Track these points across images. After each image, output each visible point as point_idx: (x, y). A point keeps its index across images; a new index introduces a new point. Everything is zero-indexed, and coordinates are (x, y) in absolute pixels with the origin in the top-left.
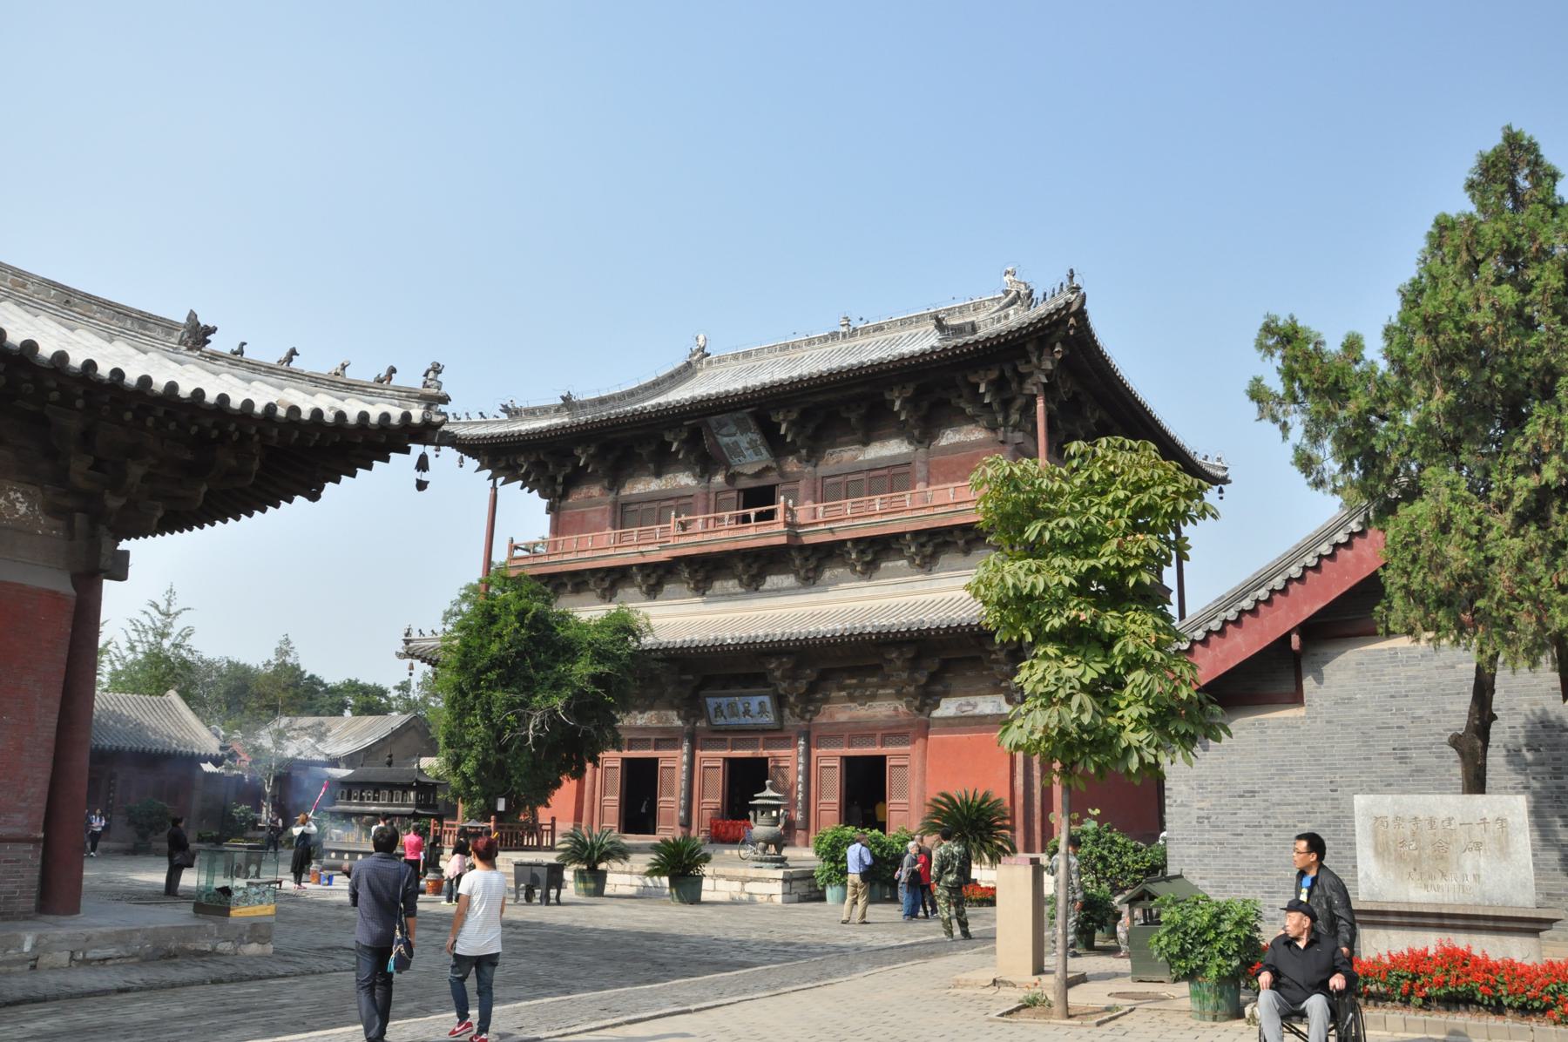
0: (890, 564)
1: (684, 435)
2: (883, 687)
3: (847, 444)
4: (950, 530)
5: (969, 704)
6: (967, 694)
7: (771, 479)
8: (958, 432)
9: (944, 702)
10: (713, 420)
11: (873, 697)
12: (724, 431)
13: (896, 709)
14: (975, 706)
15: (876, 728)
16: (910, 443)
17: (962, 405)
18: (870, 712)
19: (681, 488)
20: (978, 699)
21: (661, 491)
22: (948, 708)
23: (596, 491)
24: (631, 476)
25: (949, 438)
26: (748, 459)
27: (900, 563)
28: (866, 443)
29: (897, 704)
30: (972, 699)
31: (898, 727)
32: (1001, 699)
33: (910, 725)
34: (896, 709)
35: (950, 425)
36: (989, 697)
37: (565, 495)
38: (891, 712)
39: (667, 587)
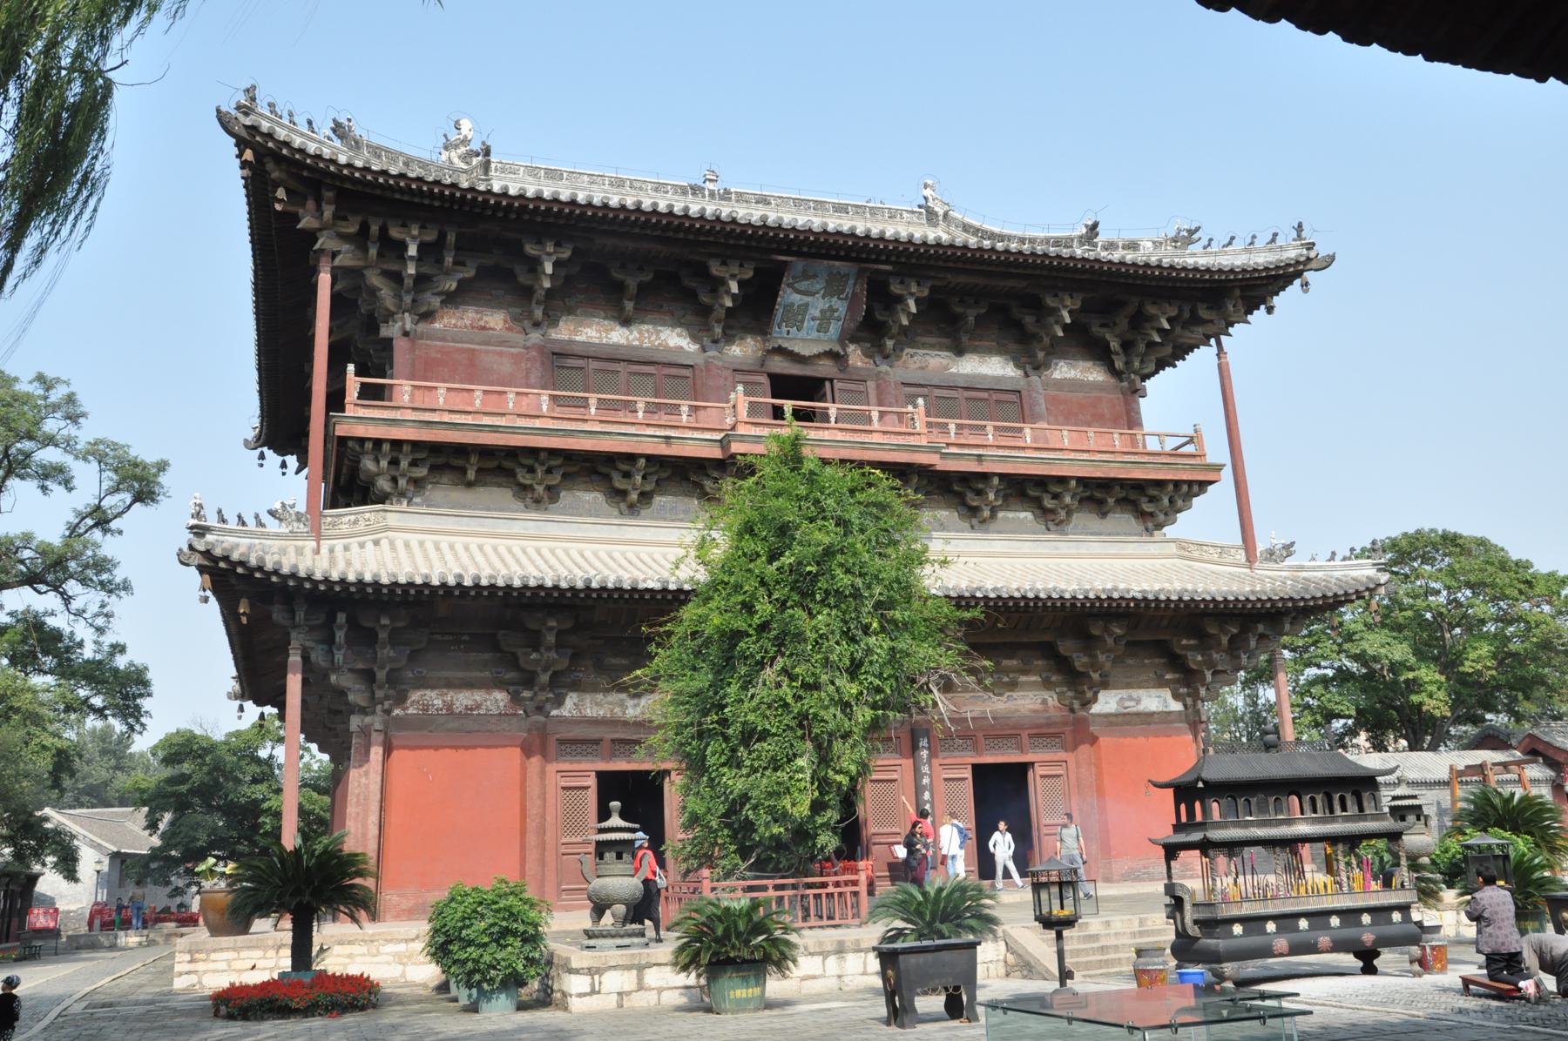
0: (1010, 515)
1: (749, 274)
2: (1025, 672)
3: (932, 347)
4: (1106, 484)
5: (1131, 698)
6: (1128, 686)
7: (825, 368)
8: (1073, 367)
9: (1102, 695)
10: (798, 264)
11: (1013, 685)
12: (804, 285)
13: (1044, 702)
14: (1138, 701)
15: (1022, 728)
16: (1017, 366)
17: (1108, 336)
18: (1011, 705)
19: (669, 350)
20: (1141, 693)
21: (629, 347)
22: (1107, 702)
23: (496, 320)
24: (570, 311)
25: (1064, 371)
26: (802, 334)
27: (1023, 515)
28: (960, 352)
29: (1046, 695)
30: (1135, 693)
31: (1049, 725)
32: (1166, 693)
33: (1065, 724)
34: (1044, 702)
35: (1064, 356)
36: (1153, 692)
37: (428, 316)
38: (1038, 707)
39: (658, 500)
